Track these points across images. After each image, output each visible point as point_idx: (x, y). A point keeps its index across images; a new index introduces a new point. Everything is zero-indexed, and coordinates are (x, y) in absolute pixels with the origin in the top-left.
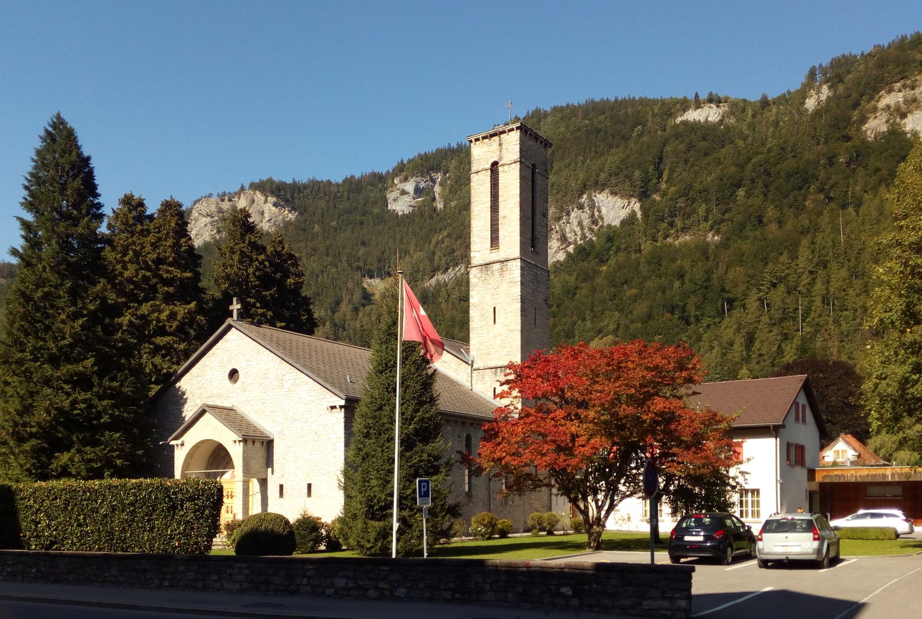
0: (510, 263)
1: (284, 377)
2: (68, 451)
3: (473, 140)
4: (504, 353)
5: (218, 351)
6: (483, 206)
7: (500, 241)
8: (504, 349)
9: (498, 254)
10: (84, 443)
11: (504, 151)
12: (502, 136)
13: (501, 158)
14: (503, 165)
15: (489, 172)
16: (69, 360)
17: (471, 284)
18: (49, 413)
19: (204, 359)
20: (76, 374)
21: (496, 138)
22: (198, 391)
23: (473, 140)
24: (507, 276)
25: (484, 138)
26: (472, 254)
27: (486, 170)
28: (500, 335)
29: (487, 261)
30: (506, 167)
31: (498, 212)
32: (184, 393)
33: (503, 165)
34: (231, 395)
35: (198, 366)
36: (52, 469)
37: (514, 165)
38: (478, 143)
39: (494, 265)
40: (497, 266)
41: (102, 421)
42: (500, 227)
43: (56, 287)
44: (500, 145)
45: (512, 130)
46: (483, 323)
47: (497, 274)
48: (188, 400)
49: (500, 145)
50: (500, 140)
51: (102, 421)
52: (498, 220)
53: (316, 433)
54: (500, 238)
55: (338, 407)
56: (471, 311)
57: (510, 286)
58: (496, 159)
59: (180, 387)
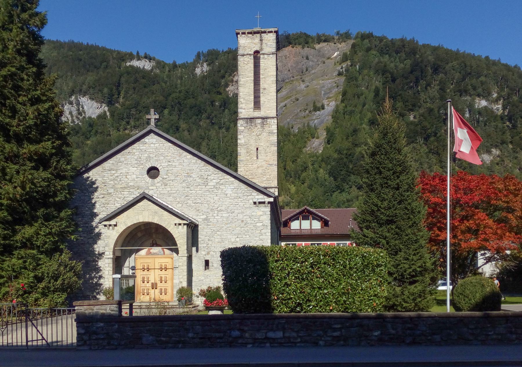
0: (269, 120)
1: (209, 177)
2: (31, 225)
3: (240, 33)
4: (265, 179)
5: (134, 151)
6: (248, 79)
7: (261, 105)
8: (264, 177)
9: (259, 113)
10: (47, 218)
11: (264, 45)
12: (262, 35)
13: (262, 49)
14: (264, 54)
15: (252, 57)
16: (31, 141)
17: (238, 130)
18: (23, 188)
19: (118, 156)
20: (36, 153)
21: (258, 35)
22: (112, 182)
23: (240, 33)
24: (267, 129)
25: (249, 33)
26: (240, 110)
27: (250, 55)
28: (262, 166)
29: (251, 116)
30: (266, 56)
31: (260, 85)
32: (94, 183)
33: (264, 54)
34: (150, 188)
35: (110, 161)
36: (16, 241)
37: (271, 56)
38: (243, 35)
39: (258, 119)
40: (259, 121)
41: (57, 199)
42: (261, 95)
43: (22, 69)
44: (261, 40)
45: (271, 32)
46: (248, 157)
47: (259, 126)
48: (99, 189)
49: (261, 40)
50: (261, 37)
51: (57, 199)
52: (259, 90)
53: (242, 221)
54: (261, 102)
55: (267, 202)
56: (239, 149)
57: (269, 135)
58: (257, 48)
59: (88, 177)
